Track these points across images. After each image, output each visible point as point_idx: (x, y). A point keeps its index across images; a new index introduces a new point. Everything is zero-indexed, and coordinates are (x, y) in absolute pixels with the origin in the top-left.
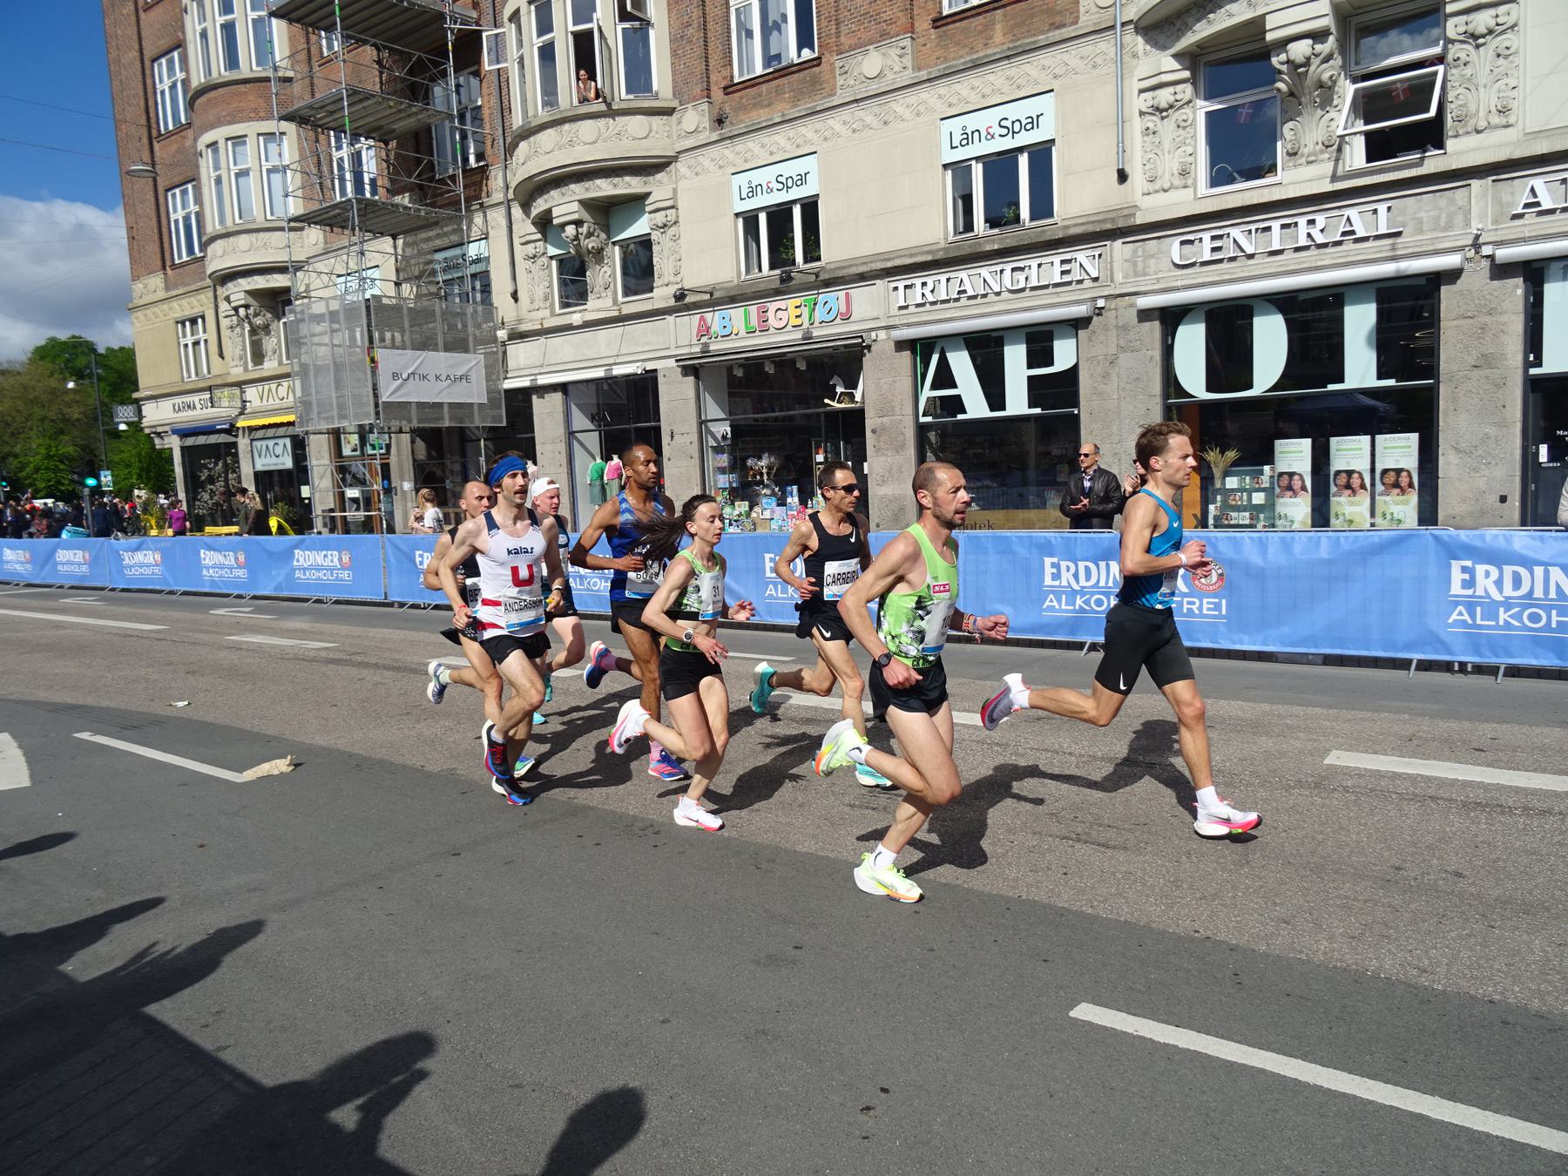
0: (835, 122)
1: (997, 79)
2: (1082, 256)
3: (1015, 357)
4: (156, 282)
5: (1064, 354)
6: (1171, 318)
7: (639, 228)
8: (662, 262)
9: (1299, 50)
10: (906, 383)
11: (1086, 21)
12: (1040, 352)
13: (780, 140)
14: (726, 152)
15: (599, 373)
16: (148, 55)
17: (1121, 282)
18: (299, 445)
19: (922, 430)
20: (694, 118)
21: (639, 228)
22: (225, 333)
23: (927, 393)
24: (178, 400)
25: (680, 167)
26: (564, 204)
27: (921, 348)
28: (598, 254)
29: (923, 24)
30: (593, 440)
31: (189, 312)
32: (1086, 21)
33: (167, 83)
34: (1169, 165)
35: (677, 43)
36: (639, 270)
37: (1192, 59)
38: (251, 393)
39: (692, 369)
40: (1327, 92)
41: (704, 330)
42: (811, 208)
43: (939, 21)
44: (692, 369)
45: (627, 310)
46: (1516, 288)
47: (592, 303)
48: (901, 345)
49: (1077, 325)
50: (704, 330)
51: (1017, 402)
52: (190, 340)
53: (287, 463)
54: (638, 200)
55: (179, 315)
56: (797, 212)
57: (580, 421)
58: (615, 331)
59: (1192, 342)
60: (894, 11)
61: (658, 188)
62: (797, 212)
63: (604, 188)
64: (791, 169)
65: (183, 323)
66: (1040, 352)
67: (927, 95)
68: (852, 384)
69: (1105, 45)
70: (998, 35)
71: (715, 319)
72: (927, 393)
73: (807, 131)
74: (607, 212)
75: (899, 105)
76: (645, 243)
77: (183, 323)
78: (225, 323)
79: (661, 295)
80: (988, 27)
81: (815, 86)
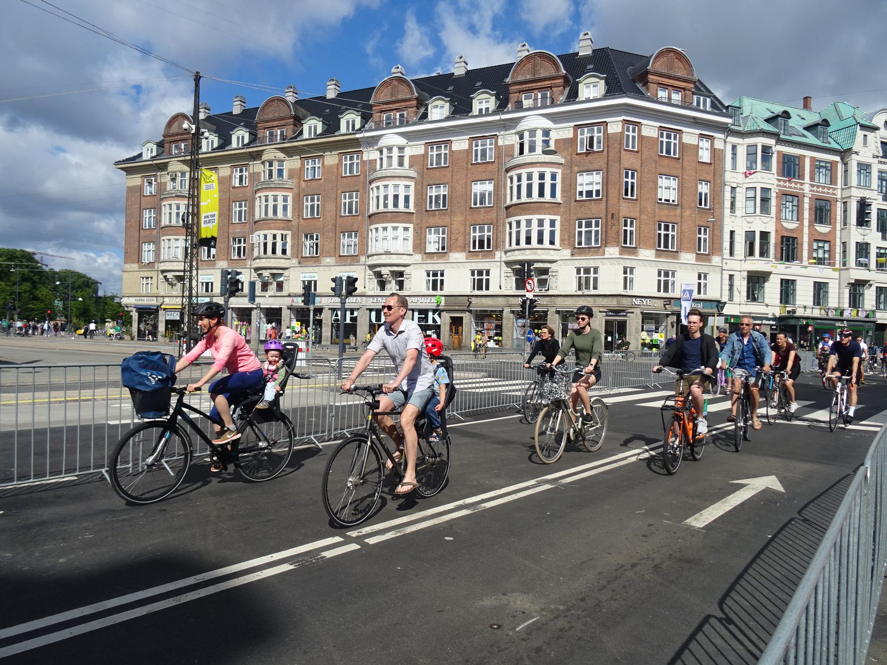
0: (321, 268)
1: (348, 268)
2: (359, 298)
3: (348, 313)
4: (135, 266)
5: (356, 314)
6: (371, 310)
7: (281, 279)
8: (285, 286)
9: (386, 276)
10: (330, 315)
11: (361, 263)
12: (352, 313)
13: (311, 269)
14: (301, 269)
15: (268, 306)
16: (142, 207)
17: (364, 303)
18: (182, 315)
19: (332, 324)
20: (295, 261)
21: (281, 279)
22: (160, 283)
23: (334, 317)
24: (138, 298)
25: (291, 269)
26: (266, 273)
27: (333, 310)
28: (271, 283)
29: (337, 256)
30: (264, 320)
31: (147, 276)
32: (361, 263)
33: (148, 216)
34: (371, 287)
35: (292, 246)
36: (280, 287)
37: (375, 273)
38: (166, 299)
39: (290, 308)
40: (390, 282)
41: (293, 301)
42: (315, 282)
43: (340, 256)
44: (290, 308)
45: (277, 295)
46: (411, 312)
47: (268, 292)
48: (330, 309)
49: (358, 309)
50: (293, 301)
51: (348, 321)
52: (145, 282)
53: (178, 318)
54: (282, 274)
55: (142, 276)
56: (313, 282)
57: (262, 316)
58: (274, 298)
59: (373, 314)
60: (332, 253)
61: (286, 273)
62: (313, 282)
63: (275, 271)
64: (313, 275)
65: (143, 278)
66: (352, 313)
67: (337, 268)
68: (321, 314)
69: (363, 267)
70: (349, 261)
71: (295, 299)
72: (334, 317)
73: (316, 268)
74: (273, 275)
75: (332, 268)
76: (282, 282)
77: (143, 278)
78: (160, 280)
79: (284, 293)
80: (347, 259)
81: (318, 260)
